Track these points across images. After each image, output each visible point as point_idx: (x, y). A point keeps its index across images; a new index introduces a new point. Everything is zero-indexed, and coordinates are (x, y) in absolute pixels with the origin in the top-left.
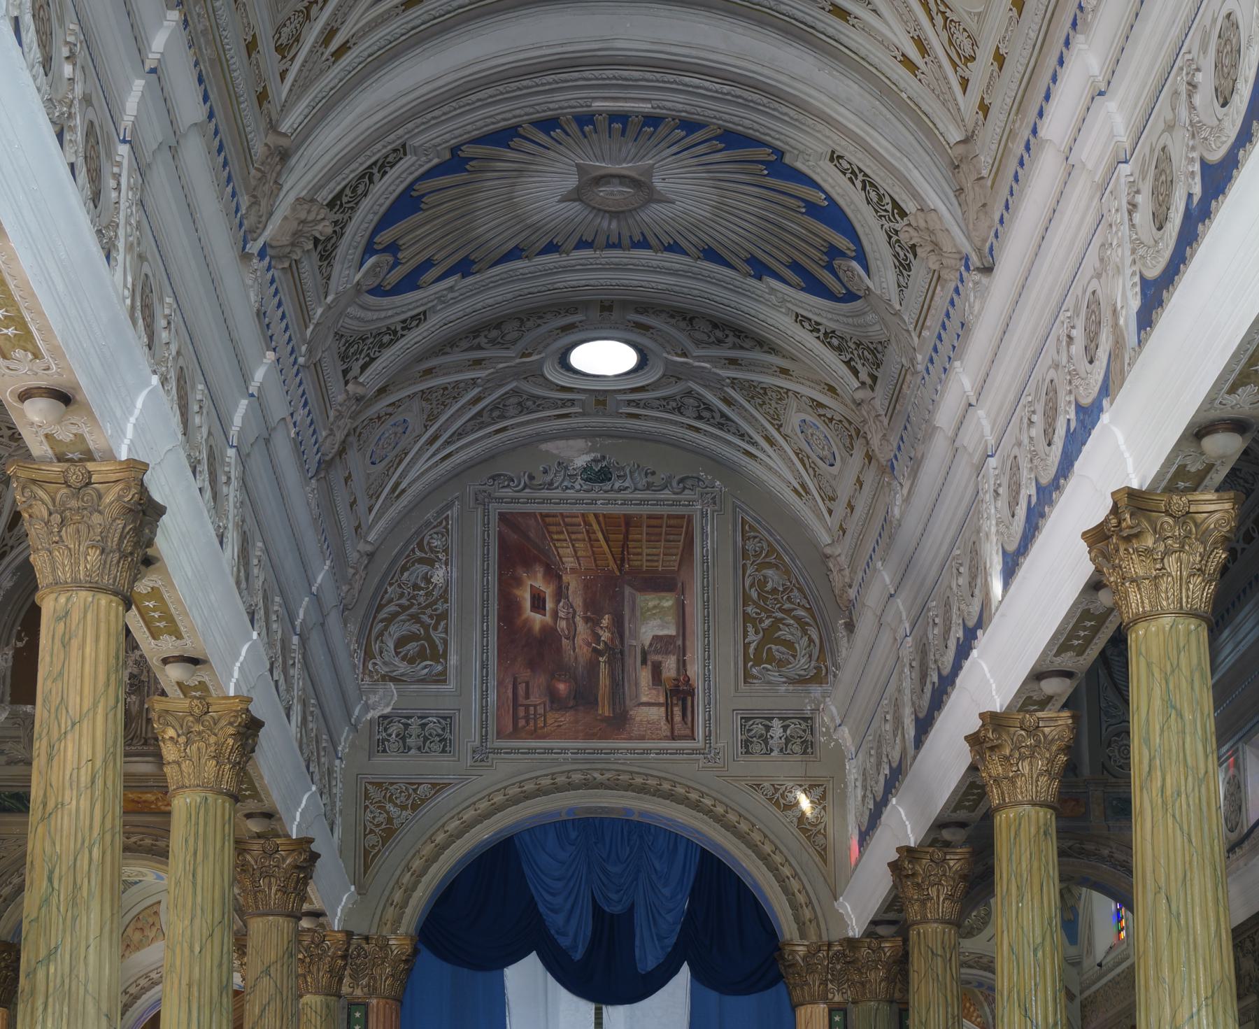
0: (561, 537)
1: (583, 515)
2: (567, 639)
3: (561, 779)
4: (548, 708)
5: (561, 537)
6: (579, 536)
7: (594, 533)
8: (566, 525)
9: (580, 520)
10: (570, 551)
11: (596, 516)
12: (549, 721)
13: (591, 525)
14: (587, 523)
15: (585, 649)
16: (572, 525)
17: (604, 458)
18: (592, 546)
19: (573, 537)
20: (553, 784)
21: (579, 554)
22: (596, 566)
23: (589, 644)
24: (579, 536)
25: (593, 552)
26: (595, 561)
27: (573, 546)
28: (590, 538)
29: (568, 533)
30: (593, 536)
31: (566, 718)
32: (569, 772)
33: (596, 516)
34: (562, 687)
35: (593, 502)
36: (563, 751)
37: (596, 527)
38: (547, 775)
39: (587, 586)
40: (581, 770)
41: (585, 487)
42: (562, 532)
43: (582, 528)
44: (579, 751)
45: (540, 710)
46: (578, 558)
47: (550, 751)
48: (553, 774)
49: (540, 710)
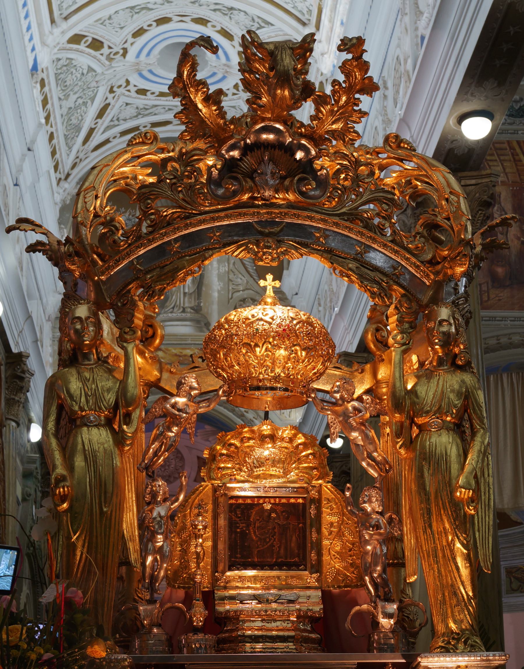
0: (493, 158)
1: (508, 142)
2: (502, 234)
3: (504, 340)
4: (490, 287)
5: (493, 158)
6: (506, 158)
7: (517, 155)
8: (496, 149)
9: (506, 145)
10: (500, 168)
11: (518, 142)
12: (492, 296)
13: (514, 149)
14: (512, 148)
15: (516, 242)
16: (501, 149)
17: (521, 99)
18: (516, 165)
19: (502, 158)
20: (498, 343)
21: (507, 170)
22: (521, 179)
23: (518, 239)
24: (506, 158)
25: (518, 170)
26: (519, 175)
27: (502, 165)
28: (514, 159)
29: (498, 155)
30: (517, 158)
31: (504, 294)
32: (510, 334)
33: (518, 142)
34: (500, 270)
35: (516, 132)
36: (504, 319)
37: (518, 150)
38: (493, 337)
39: (515, 195)
40: (519, 333)
41: (508, 121)
42: (492, 155)
43: (508, 151)
44: (516, 319)
45: (484, 288)
46: (506, 174)
47: (494, 319)
48: (498, 336)
49: (484, 288)
